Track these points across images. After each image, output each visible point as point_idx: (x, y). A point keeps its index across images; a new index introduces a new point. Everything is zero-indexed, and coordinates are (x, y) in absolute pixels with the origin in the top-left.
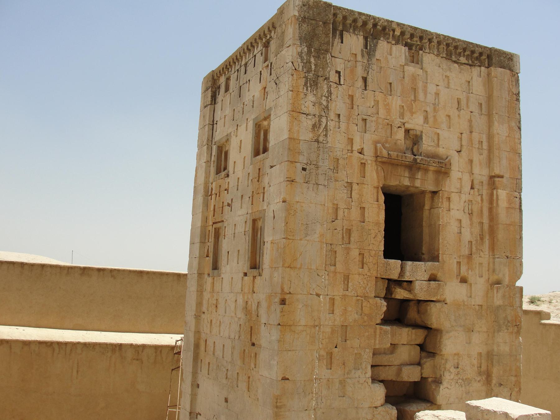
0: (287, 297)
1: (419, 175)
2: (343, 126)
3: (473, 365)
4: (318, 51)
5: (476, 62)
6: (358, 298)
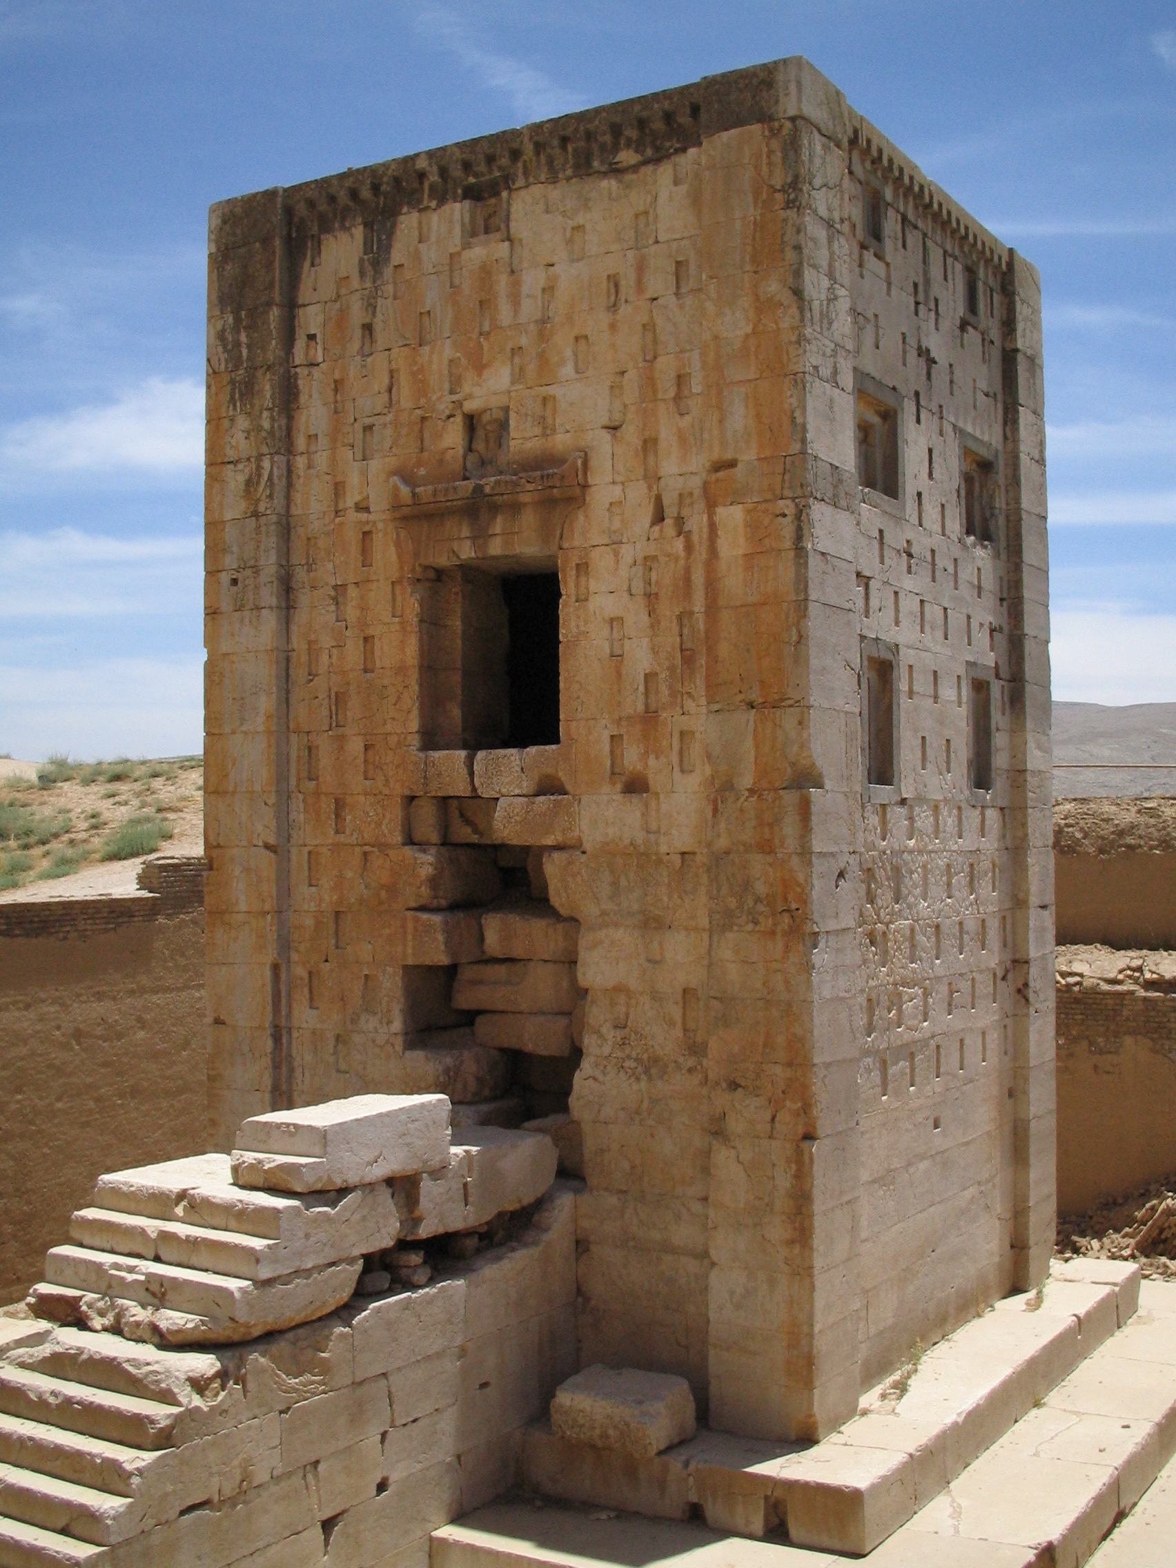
0: (215, 853)
1: (498, 526)
2: (322, 459)
3: (672, 1024)
4: (252, 313)
5: (668, 144)
6: (367, 848)
